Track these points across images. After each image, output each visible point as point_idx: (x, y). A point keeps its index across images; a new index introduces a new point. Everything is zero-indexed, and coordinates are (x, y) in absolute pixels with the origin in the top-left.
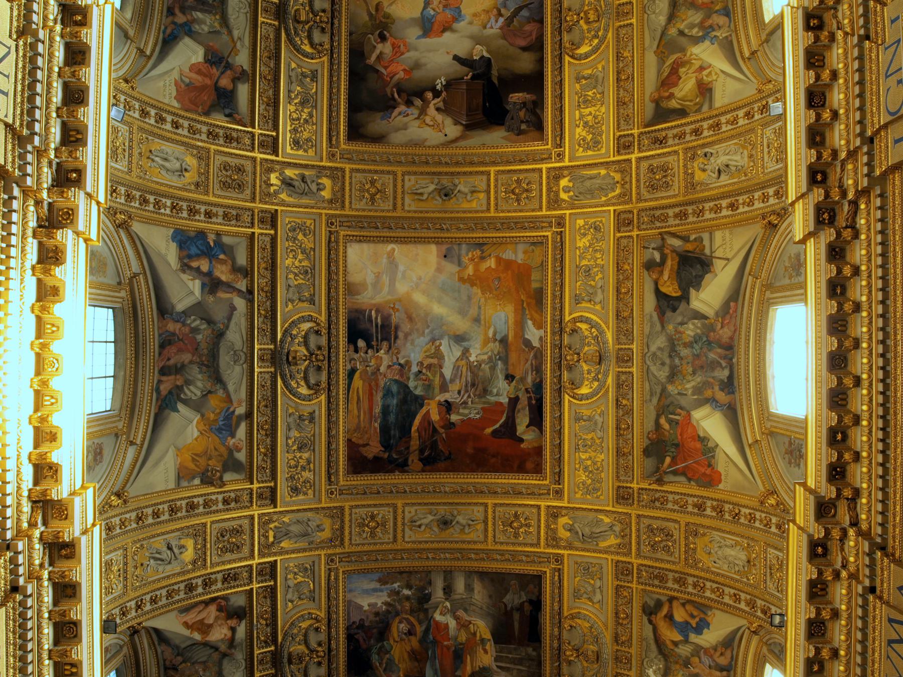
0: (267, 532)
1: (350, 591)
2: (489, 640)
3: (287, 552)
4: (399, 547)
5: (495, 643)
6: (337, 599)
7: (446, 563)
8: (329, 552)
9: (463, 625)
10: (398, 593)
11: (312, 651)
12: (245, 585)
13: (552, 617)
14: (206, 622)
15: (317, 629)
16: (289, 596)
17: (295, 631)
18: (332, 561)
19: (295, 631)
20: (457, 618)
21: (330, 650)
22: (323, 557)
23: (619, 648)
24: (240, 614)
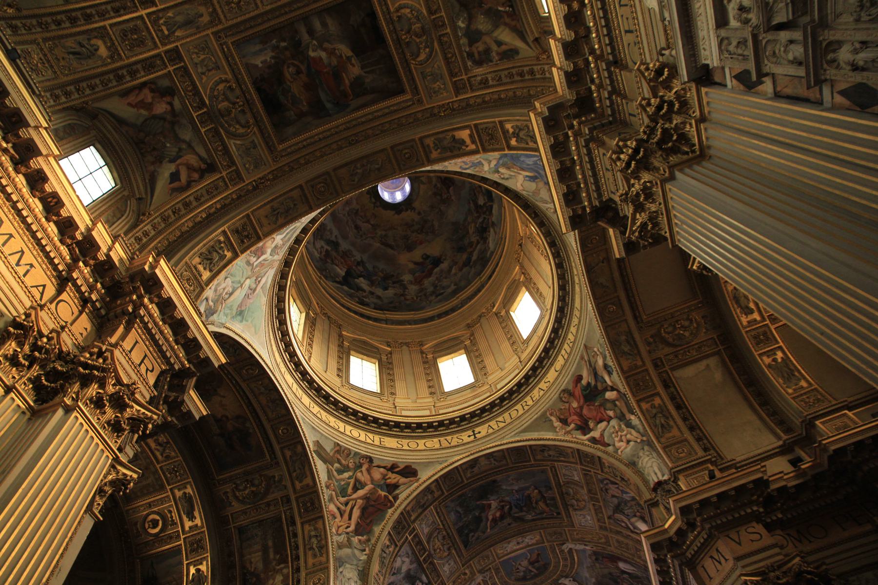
0: (160, 26)
1: (244, 57)
2: (352, 56)
3: (183, 39)
4: (262, 11)
5: (357, 56)
6: (236, 64)
7: (301, 11)
8: (215, 29)
9: (331, 53)
10: (278, 47)
11: (234, 104)
12: (162, 70)
13: (385, 19)
14: (146, 101)
15: (230, 87)
16: (200, 70)
17: (216, 93)
18: (220, 37)
19: (216, 93)
20: (325, 50)
21: (248, 101)
22: (211, 35)
23: (434, 17)
24: (170, 92)
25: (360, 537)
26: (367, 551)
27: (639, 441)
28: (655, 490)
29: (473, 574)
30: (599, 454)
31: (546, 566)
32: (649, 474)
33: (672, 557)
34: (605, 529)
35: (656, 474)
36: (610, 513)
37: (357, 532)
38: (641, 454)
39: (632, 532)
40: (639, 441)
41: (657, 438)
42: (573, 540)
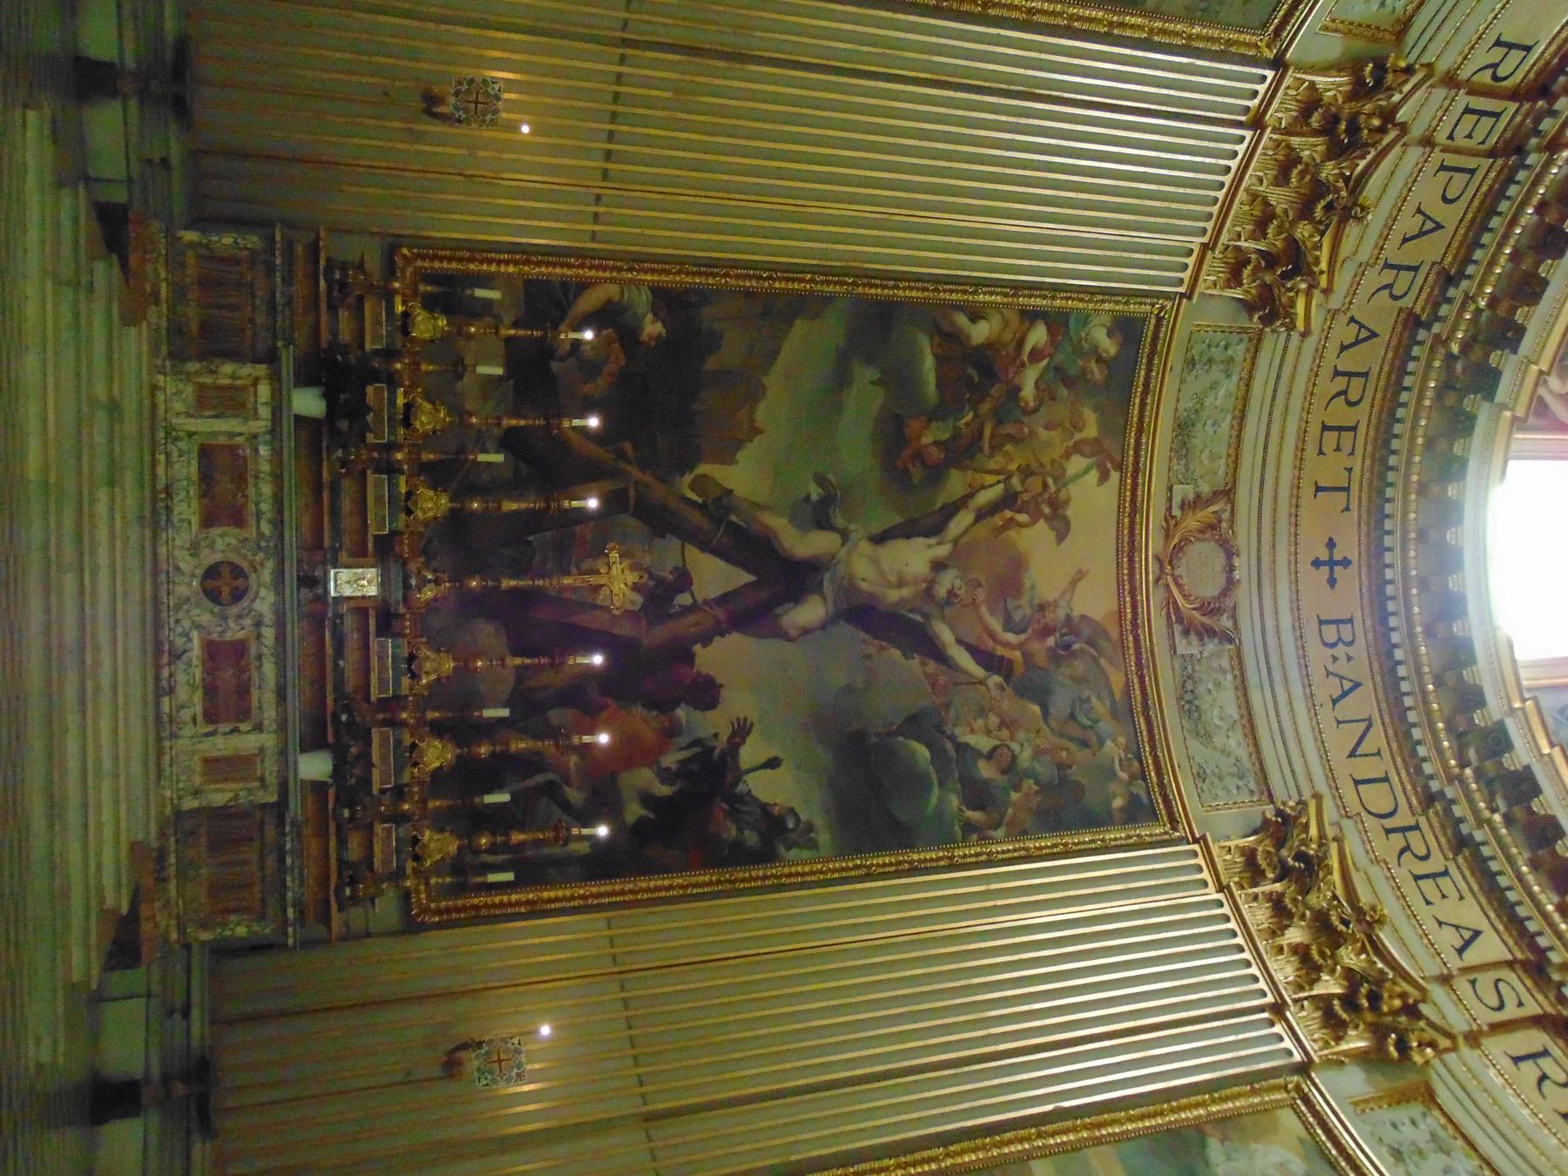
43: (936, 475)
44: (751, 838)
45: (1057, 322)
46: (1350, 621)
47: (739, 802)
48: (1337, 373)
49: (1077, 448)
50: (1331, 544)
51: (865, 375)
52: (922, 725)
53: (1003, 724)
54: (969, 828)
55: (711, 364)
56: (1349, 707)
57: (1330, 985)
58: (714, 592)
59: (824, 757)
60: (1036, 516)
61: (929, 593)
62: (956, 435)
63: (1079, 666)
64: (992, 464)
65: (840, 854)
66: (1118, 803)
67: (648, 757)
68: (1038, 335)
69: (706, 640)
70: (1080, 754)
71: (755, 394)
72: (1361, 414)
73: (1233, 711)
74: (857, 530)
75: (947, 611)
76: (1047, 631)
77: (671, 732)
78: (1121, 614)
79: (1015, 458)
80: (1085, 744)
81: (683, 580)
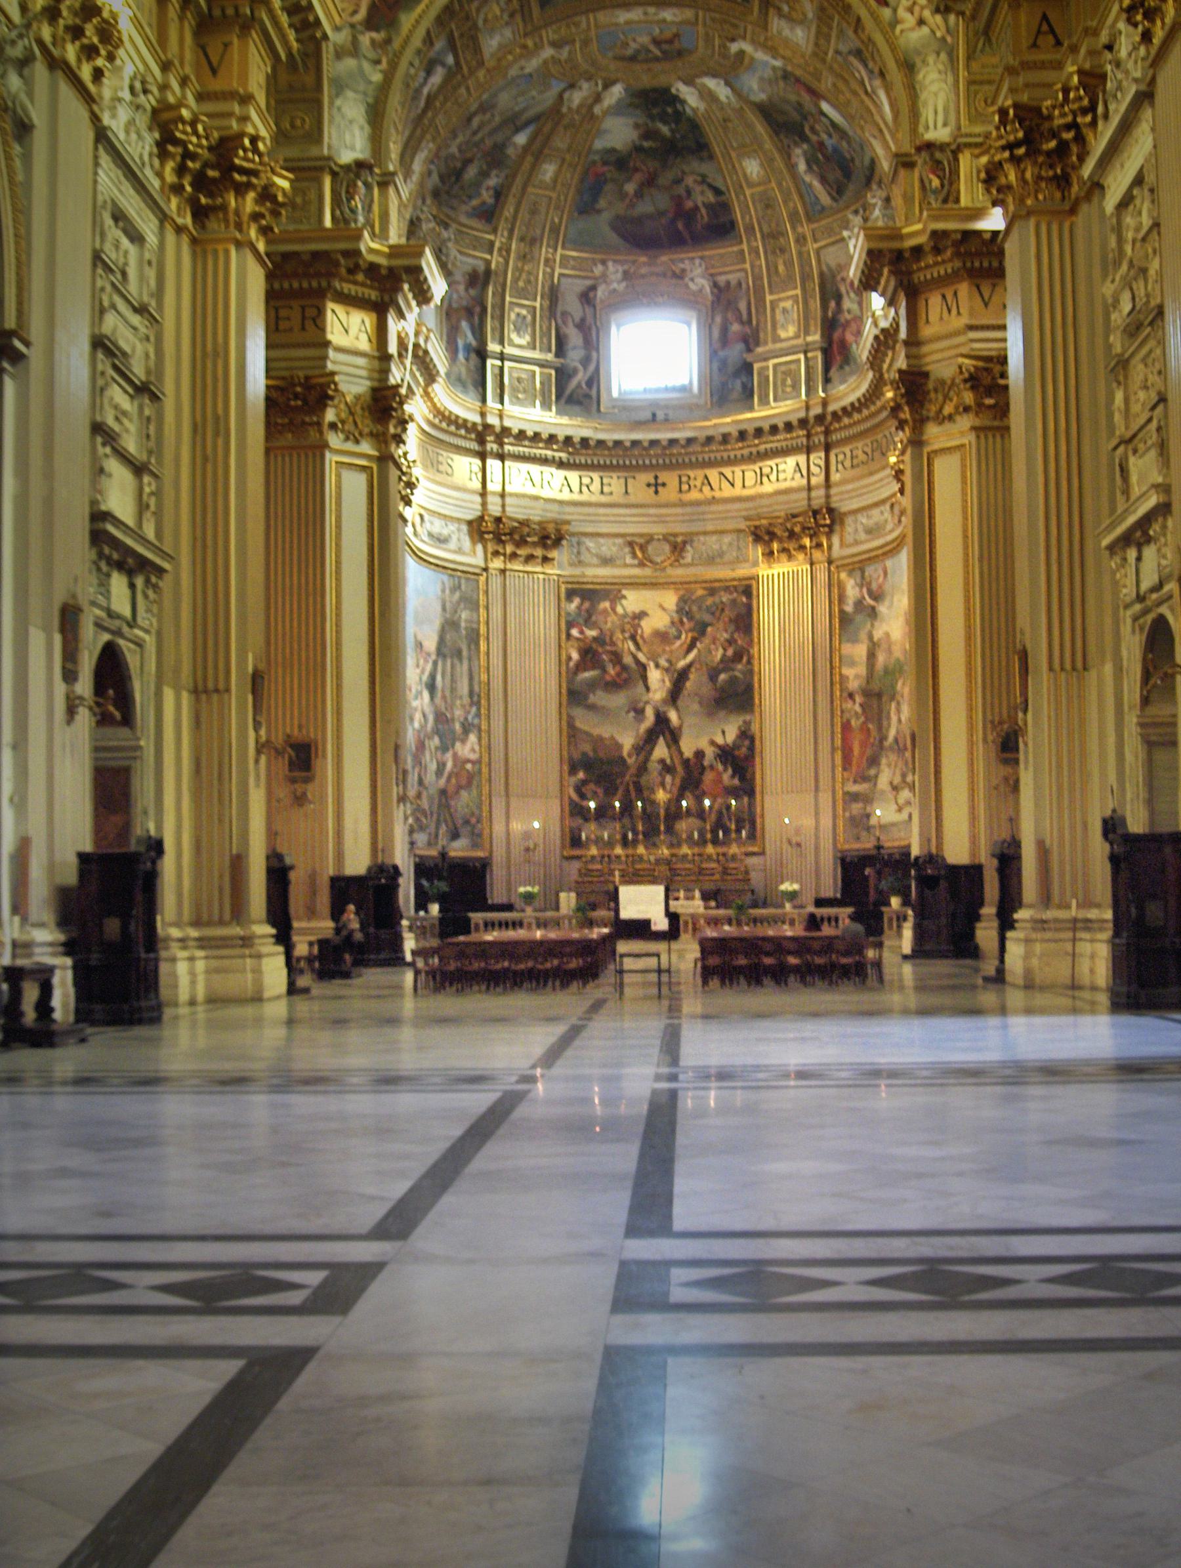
25: (374, 35)
26: (384, 64)
27: (939, 34)
28: (919, 149)
29: (539, 47)
30: (864, 13)
31: (680, 54)
32: (925, 104)
33: (890, 272)
34: (824, 61)
35: (936, 113)
36: (844, 48)
37: (371, 23)
38: (931, 59)
39: (866, 92)
40: (939, 34)
41: (969, 58)
42: (753, 42)
43: (625, 668)
44: (747, 743)
45: (570, 625)
46: (680, 477)
47: (736, 746)
48: (581, 491)
49: (614, 609)
50: (649, 485)
51: (592, 699)
52: (713, 676)
53: (714, 643)
54: (749, 662)
55: (591, 754)
56: (715, 485)
57: (807, 542)
58: (666, 750)
59: (722, 714)
60: (639, 625)
61: (667, 670)
62: (611, 661)
63: (695, 608)
64: (620, 645)
65: (752, 711)
66: (744, 599)
67: (719, 775)
68: (575, 632)
69: (681, 753)
70: (727, 612)
71: (601, 738)
72: (596, 476)
73: (714, 538)
74: (645, 698)
75: (674, 661)
76: (682, 622)
77: (712, 767)
78: (677, 590)
79: (619, 635)
80: (723, 610)
81: (662, 761)
